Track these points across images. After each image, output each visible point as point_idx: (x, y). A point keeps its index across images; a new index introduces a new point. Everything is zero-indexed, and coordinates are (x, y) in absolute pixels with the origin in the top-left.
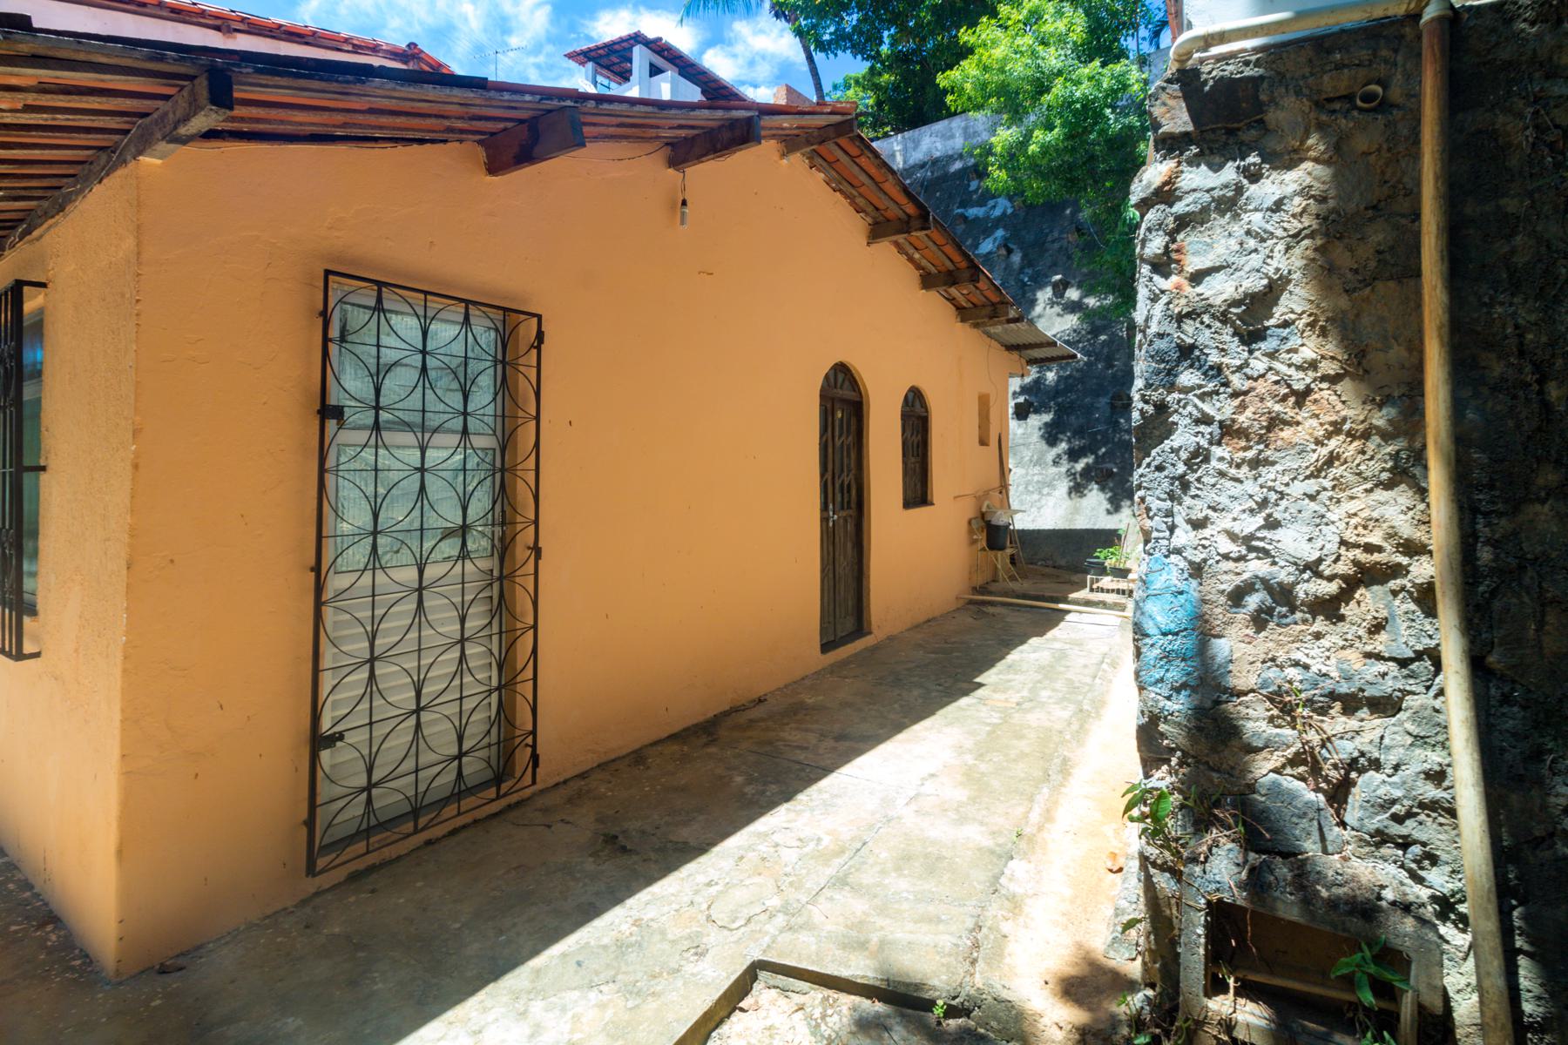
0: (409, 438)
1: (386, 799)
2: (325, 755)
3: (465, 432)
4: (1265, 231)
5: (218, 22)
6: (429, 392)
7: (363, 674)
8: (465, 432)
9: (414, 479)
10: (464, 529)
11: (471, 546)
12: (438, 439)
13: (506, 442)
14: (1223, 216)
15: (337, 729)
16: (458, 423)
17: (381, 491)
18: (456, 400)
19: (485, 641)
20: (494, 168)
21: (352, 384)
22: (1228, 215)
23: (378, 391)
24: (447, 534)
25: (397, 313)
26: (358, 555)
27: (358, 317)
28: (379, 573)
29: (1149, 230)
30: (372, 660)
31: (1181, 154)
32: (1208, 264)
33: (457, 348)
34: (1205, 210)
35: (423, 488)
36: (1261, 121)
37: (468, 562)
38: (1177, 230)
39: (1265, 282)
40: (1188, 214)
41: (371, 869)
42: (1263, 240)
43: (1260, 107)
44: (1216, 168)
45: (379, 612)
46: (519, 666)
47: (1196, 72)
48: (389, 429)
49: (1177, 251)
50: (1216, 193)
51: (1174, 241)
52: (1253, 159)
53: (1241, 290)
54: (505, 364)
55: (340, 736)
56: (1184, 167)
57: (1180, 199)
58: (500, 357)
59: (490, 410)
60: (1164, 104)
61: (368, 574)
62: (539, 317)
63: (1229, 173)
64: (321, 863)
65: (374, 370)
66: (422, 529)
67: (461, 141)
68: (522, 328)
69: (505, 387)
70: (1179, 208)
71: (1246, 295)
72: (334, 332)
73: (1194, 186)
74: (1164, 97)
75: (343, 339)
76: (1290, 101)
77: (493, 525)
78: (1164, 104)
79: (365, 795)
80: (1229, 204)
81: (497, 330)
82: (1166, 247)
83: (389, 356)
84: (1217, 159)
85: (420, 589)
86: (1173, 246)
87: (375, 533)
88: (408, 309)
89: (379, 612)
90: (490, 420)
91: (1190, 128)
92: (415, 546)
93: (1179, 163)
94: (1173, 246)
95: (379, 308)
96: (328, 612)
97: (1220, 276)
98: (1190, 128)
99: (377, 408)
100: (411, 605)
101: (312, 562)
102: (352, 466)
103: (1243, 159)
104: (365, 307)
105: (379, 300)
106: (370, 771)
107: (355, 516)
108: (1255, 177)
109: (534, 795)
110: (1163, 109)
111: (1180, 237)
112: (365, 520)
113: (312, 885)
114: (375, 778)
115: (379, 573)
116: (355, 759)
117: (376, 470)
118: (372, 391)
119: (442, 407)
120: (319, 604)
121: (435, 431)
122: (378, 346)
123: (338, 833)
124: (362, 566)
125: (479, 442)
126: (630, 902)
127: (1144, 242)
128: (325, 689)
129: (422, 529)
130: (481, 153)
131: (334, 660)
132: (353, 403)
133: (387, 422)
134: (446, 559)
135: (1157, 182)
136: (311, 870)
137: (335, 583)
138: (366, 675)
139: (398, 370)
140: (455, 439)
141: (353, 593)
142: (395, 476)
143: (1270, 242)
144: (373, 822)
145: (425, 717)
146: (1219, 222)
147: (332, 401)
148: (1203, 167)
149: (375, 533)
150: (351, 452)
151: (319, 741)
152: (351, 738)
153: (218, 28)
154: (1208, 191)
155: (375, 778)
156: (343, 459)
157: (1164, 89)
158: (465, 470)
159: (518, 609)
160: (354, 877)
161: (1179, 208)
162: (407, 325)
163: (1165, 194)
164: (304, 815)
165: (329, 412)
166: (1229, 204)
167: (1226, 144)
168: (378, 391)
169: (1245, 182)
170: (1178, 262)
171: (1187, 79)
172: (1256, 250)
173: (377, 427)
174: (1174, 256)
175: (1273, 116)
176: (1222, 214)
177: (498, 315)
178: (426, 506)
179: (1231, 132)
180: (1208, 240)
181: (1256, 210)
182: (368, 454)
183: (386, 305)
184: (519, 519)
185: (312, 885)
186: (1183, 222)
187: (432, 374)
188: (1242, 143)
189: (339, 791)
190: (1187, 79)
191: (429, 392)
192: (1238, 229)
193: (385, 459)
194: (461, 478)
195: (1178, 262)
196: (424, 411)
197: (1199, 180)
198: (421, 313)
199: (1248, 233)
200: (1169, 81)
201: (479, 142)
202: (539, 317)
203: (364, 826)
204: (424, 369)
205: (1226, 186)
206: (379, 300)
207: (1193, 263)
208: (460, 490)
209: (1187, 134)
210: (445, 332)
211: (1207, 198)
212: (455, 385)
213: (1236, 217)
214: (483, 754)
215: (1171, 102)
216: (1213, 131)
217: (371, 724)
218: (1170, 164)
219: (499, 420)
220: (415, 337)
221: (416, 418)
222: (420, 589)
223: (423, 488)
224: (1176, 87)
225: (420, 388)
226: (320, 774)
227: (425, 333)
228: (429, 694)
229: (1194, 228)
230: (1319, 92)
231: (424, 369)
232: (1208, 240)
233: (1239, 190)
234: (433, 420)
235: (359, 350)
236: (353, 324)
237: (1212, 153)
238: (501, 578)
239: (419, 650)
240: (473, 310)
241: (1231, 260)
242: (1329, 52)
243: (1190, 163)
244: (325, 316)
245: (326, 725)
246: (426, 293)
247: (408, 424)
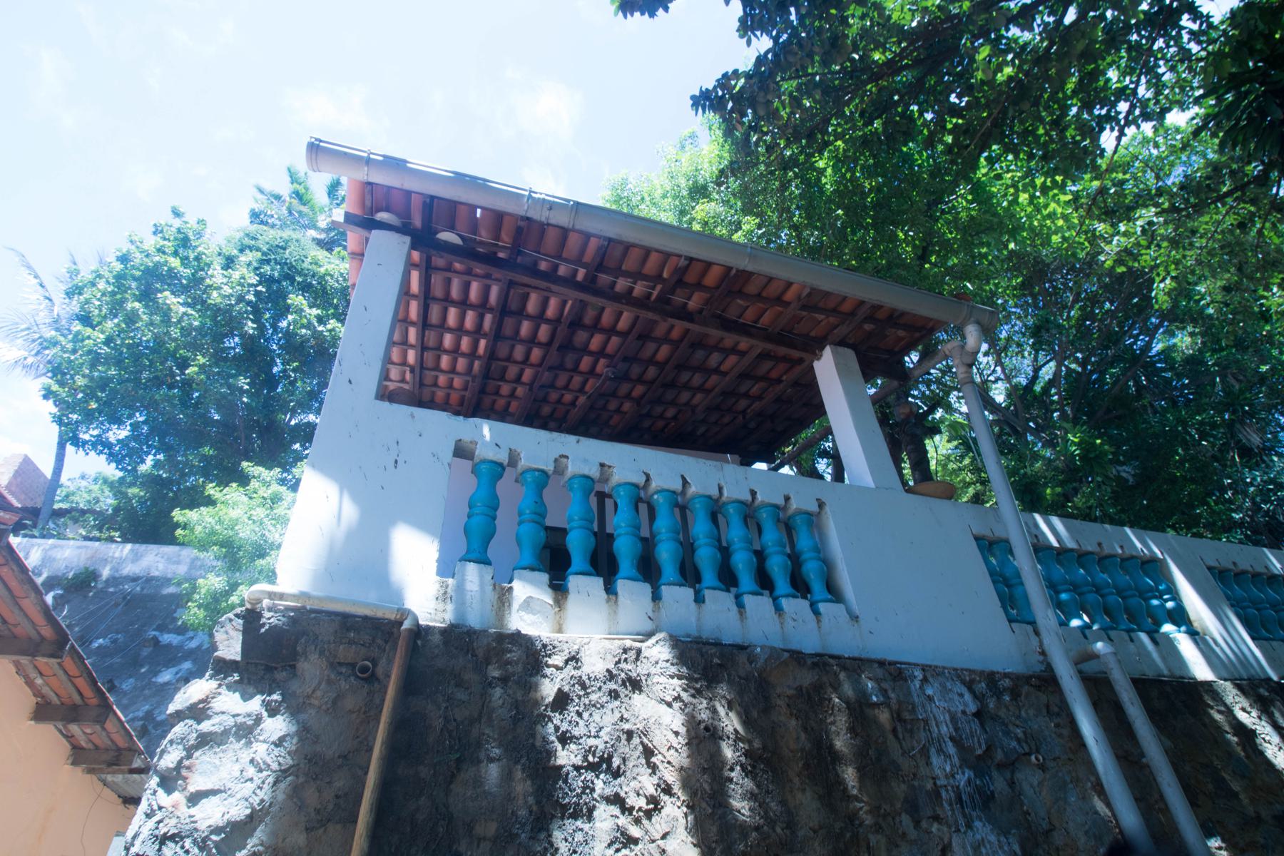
4: (264, 763)
14: (238, 741)
22: (243, 741)
29: (171, 742)
31: (225, 678)
32: (209, 786)
34: (226, 732)
36: (293, 667)
38: (197, 747)
39: (248, 811)
40: (211, 733)
42: (261, 771)
43: (294, 656)
44: (246, 697)
47: (260, 615)
49: (188, 768)
50: (240, 720)
51: (189, 756)
52: (276, 697)
53: (227, 817)
56: (223, 690)
57: (209, 717)
60: (227, 633)
63: (255, 705)
70: (206, 726)
71: (229, 823)
73: (224, 709)
74: (229, 626)
76: (314, 657)
78: (227, 633)
80: (246, 731)
82: (180, 762)
84: (251, 690)
86: (186, 763)
91: (238, 658)
93: (220, 685)
94: (186, 763)
97: (214, 800)
98: (238, 658)
103: (269, 695)
108: (273, 712)
110: (225, 636)
111: (197, 754)
127: (163, 752)
135: (195, 699)
143: (265, 773)
146: (234, 745)
148: (237, 694)
154: (234, 716)
157: (231, 620)
161: (206, 726)
163: (198, 712)
166: (246, 731)
167: (263, 678)
169: (265, 714)
170: (185, 779)
171: (251, 617)
172: (251, 779)
174: (184, 772)
175: (303, 666)
176: (239, 739)
179: (269, 669)
180: (217, 762)
181: (264, 741)
186: (205, 740)
188: (274, 680)
190: (251, 617)
192: (246, 756)
195: (185, 779)
197: (232, 705)
199: (252, 761)
200: (237, 616)
205: (249, 715)
207: (197, 782)
209: (235, 662)
211: (230, 722)
213: (249, 743)
215: (232, 633)
216: (256, 665)
218: (213, 684)
224: (241, 621)
229: (212, 747)
230: (335, 656)
232: (217, 762)
233: (258, 720)
237: (249, 683)
241: (229, 785)
242: (348, 630)
243: (229, 687)
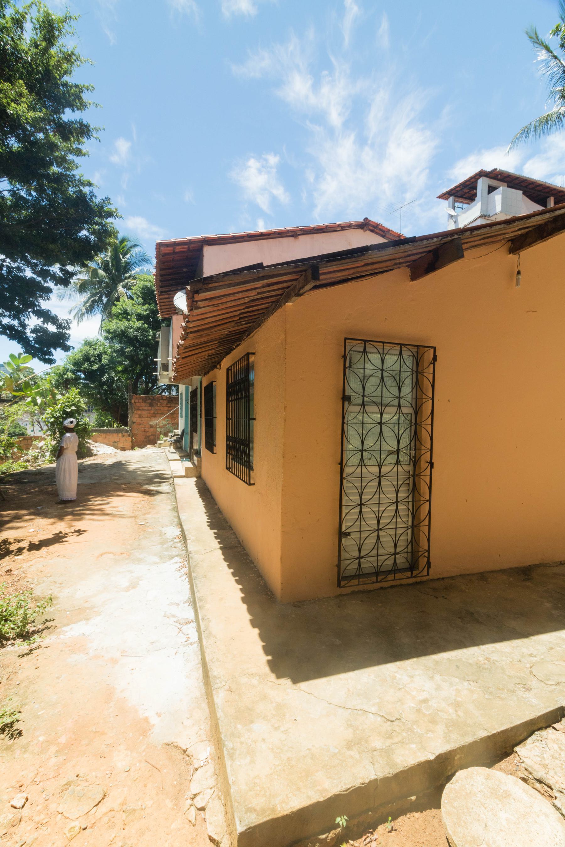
0: (376, 409)
1: (368, 564)
2: (343, 540)
3: (399, 406)
5: (293, 233)
6: (384, 388)
7: (357, 510)
8: (399, 406)
9: (380, 428)
10: (398, 451)
11: (401, 459)
12: (388, 409)
13: (417, 411)
15: (348, 531)
16: (396, 402)
17: (365, 433)
18: (395, 391)
19: (406, 504)
20: (415, 276)
21: (354, 385)
23: (364, 388)
24: (390, 453)
25: (371, 353)
26: (356, 460)
27: (356, 357)
28: (363, 467)
30: (361, 505)
33: (397, 367)
35: (381, 432)
37: (400, 467)
41: (360, 592)
45: (364, 484)
46: (422, 518)
48: (367, 405)
54: (417, 373)
55: (348, 534)
58: (415, 369)
59: (410, 396)
61: (360, 467)
62: (435, 348)
64: (343, 583)
65: (362, 378)
66: (381, 450)
67: (399, 268)
68: (426, 354)
69: (417, 385)
72: (347, 365)
75: (350, 367)
77: (410, 450)
79: (358, 560)
81: (414, 356)
83: (368, 372)
85: (380, 477)
87: (362, 451)
88: (376, 351)
89: (364, 484)
90: (410, 400)
92: (377, 456)
95: (365, 351)
96: (344, 481)
99: (364, 396)
100: (376, 483)
101: (339, 461)
102: (353, 421)
104: (360, 352)
105: (365, 349)
106: (360, 550)
107: (354, 442)
109: (428, 580)
112: (358, 444)
113: (339, 591)
114: (362, 554)
115: (363, 467)
116: (354, 545)
117: (363, 423)
118: (361, 388)
119: (388, 394)
120: (342, 479)
121: (386, 406)
122: (364, 369)
123: (348, 573)
124: (356, 464)
125: (405, 410)
126: (482, 647)
128: (343, 515)
129: (381, 450)
130: (408, 271)
131: (346, 502)
132: (353, 394)
133: (367, 402)
134: (390, 464)
136: (339, 585)
137: (348, 470)
138: (359, 510)
139: (371, 378)
140: (395, 409)
141: (354, 475)
142: (369, 426)
144: (361, 573)
145: (381, 533)
147: (346, 394)
149: (362, 451)
150: (353, 415)
151: (342, 534)
152: (353, 535)
153: (292, 236)
155: (362, 554)
156: (350, 418)
158: (399, 424)
159: (422, 491)
160: (353, 593)
162: (375, 358)
164: (336, 563)
165: (346, 399)
168: (364, 388)
173: (363, 404)
177: (414, 349)
178: (382, 439)
182: (360, 417)
183: (367, 350)
184: (423, 448)
185: (339, 591)
187: (385, 379)
189: (347, 556)
191: (384, 388)
193: (366, 419)
194: (397, 427)
196: (382, 397)
198: (381, 352)
201: (407, 266)
202: (435, 348)
203: (357, 573)
204: (382, 378)
206: (365, 349)
208: (397, 433)
210: (391, 360)
212: (394, 384)
214: (405, 555)
217: (360, 531)
219: (414, 400)
220: (378, 363)
221: (378, 400)
222: (380, 477)
223: (381, 432)
225: (380, 387)
226: (342, 548)
227: (383, 361)
228: (382, 523)
231: (382, 378)
234: (385, 401)
235: (356, 370)
236: (354, 360)
238: (414, 476)
239: (379, 503)
240: (403, 348)
244: (344, 357)
245: (343, 529)
246: (383, 343)
247: (375, 403)
